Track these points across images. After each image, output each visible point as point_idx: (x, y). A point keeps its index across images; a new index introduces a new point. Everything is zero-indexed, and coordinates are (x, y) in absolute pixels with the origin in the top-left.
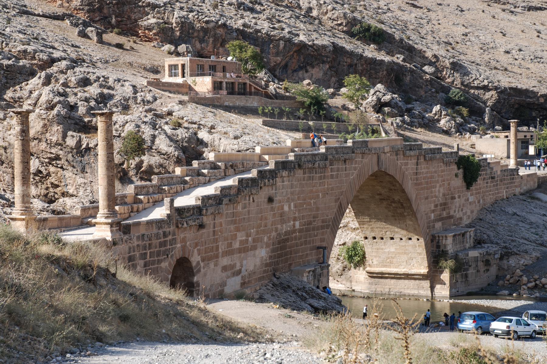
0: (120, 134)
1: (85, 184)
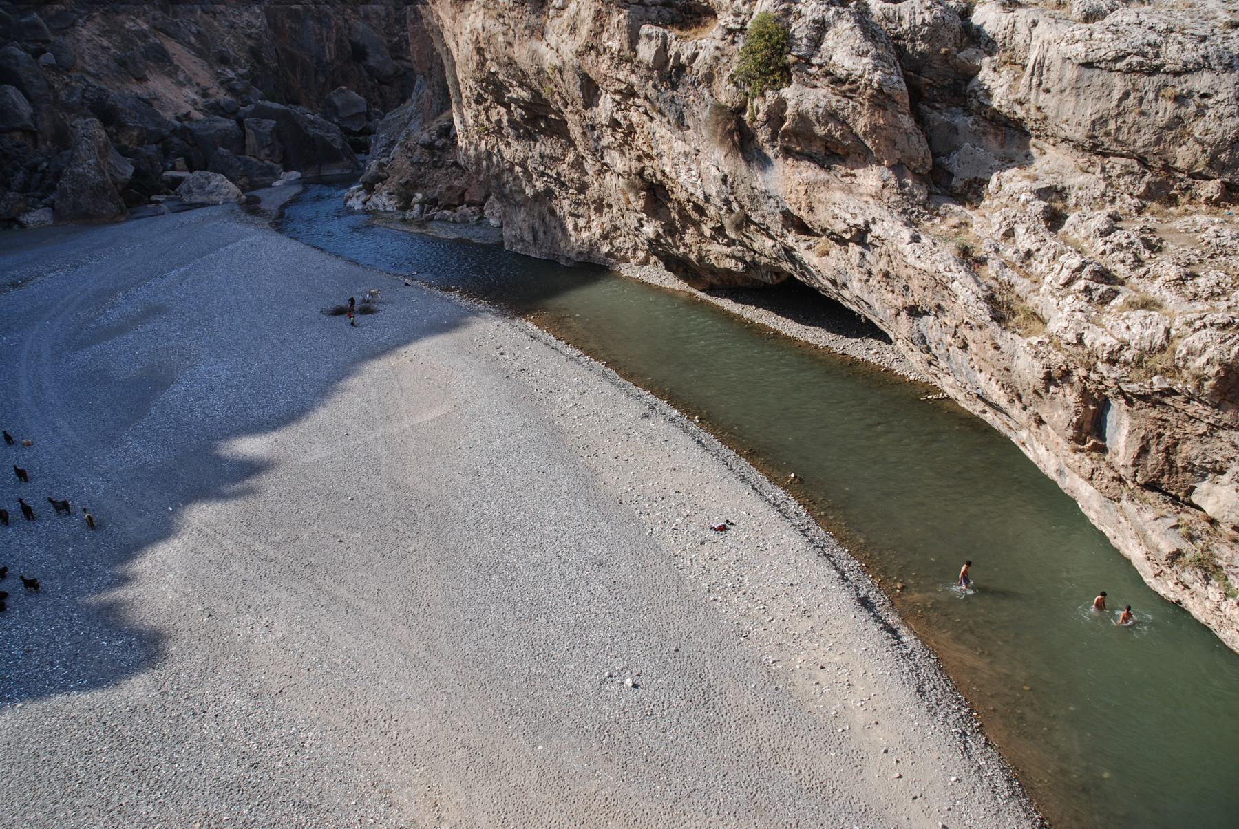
0: (744, 23)
1: (686, 155)
